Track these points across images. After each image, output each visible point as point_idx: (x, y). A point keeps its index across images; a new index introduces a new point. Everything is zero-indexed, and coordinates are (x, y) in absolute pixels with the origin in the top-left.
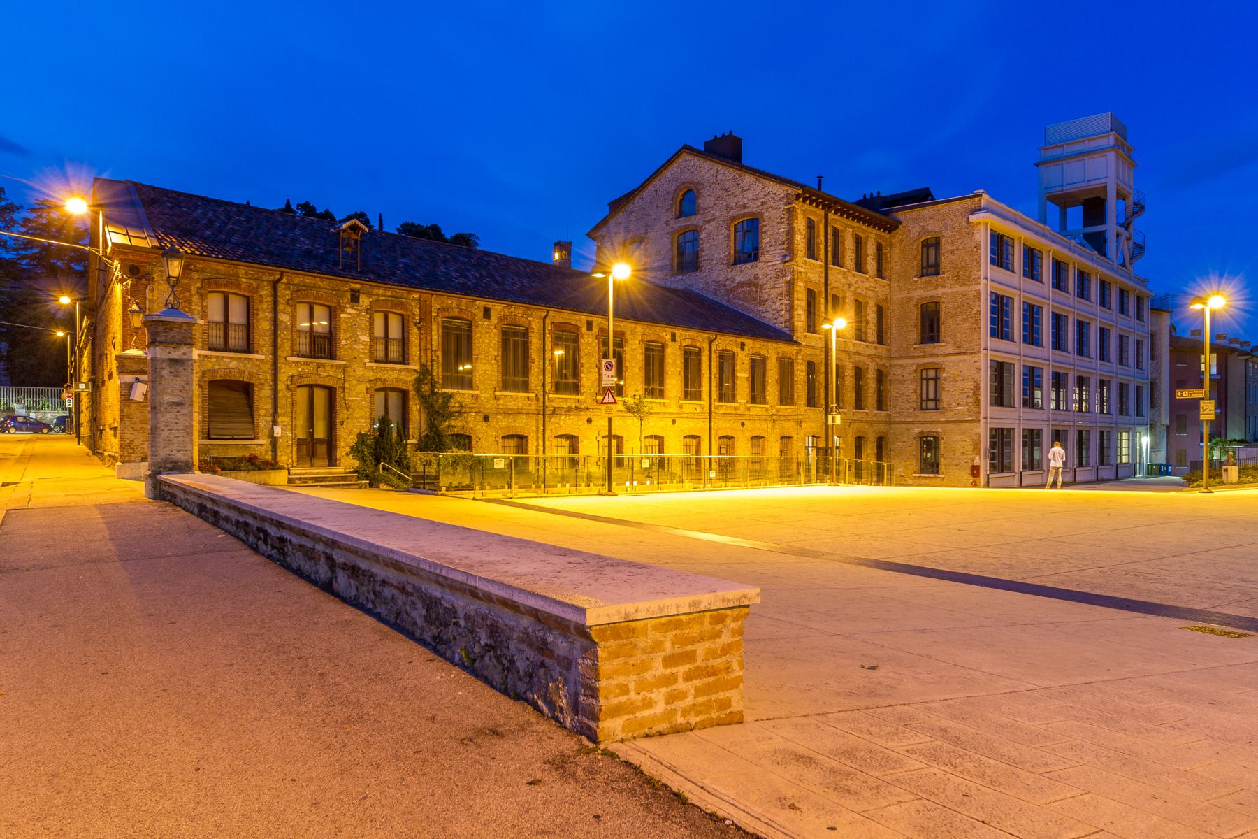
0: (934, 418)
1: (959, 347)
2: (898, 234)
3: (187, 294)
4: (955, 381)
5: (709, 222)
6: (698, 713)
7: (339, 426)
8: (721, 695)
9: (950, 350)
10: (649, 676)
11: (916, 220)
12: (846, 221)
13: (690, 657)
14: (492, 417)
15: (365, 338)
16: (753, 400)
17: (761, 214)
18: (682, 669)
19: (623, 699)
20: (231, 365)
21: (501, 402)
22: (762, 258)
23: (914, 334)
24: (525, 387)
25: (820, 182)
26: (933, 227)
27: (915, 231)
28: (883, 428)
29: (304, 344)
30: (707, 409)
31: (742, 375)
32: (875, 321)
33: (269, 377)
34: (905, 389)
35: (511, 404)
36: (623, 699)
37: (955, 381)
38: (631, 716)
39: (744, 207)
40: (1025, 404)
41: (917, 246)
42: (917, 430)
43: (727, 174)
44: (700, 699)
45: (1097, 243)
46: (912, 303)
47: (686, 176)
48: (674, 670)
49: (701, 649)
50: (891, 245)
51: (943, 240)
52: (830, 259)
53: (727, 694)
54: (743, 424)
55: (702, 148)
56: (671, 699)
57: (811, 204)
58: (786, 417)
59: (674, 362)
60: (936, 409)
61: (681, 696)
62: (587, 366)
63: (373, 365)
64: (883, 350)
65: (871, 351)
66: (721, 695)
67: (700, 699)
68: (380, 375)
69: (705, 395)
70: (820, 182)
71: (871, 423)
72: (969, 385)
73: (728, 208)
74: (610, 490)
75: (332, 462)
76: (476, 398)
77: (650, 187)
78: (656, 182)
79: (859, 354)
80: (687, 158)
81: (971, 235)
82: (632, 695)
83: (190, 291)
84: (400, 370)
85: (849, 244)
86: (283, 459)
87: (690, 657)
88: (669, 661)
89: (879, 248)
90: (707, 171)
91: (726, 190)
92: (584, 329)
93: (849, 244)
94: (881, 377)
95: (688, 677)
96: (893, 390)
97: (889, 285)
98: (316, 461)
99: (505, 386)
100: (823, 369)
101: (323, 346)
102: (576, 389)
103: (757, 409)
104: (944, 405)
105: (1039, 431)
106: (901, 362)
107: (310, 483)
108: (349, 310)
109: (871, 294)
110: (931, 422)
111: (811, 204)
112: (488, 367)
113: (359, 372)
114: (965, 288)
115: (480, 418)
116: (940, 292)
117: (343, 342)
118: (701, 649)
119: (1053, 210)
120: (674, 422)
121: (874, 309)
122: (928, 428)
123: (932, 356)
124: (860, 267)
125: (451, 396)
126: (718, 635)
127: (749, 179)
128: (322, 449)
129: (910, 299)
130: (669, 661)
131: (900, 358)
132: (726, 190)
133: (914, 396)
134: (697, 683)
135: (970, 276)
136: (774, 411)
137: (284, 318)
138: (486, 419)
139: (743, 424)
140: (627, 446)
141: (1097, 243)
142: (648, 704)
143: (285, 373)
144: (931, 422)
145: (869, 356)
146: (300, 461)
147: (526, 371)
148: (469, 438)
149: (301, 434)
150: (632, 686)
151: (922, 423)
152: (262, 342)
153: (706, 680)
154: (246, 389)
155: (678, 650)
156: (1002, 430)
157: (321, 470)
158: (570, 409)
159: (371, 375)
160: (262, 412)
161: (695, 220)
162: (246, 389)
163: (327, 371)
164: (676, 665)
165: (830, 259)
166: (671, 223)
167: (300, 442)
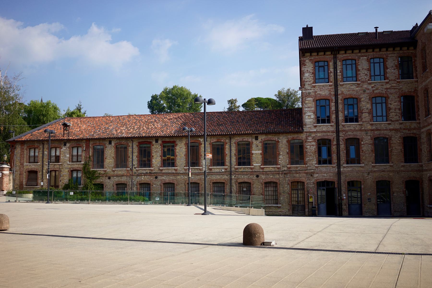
14: (112, 177)
20: (33, 167)
21: (116, 172)
31: (257, 152)
35: (120, 173)
50: (416, 57)
62: (155, 157)
64: (408, 123)
65: (397, 126)
68: (72, 166)
69: (227, 163)
76: (105, 171)
79: (380, 130)
84: (79, 164)
92: (154, 142)
99: (117, 166)
100: (335, 143)
102: (173, 164)
109: (393, 91)
113: (66, 166)
115: (107, 178)
125: (96, 171)
138: (109, 178)
139: (257, 176)
145: (391, 130)
148: (103, 185)
158: (147, 173)
159: (70, 166)
163: (57, 166)
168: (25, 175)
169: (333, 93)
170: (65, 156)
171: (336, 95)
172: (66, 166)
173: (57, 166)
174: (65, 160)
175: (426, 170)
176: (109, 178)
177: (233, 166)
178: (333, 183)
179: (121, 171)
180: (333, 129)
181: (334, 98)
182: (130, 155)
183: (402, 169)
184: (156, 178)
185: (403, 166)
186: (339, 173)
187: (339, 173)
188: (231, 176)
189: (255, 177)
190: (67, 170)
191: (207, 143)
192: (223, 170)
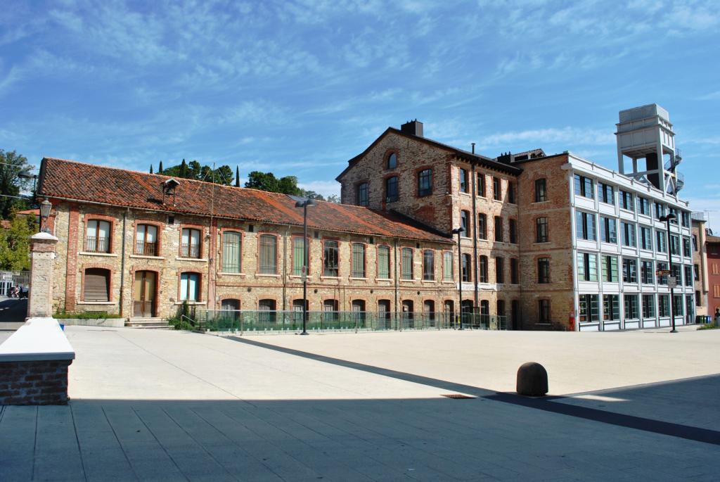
0: (546, 289)
1: (559, 245)
2: (522, 177)
3: (76, 222)
4: (557, 265)
5: (404, 171)
6: (43, 399)
7: (159, 294)
8: (56, 394)
9: (553, 246)
10: (18, 383)
11: (532, 169)
12: (487, 170)
13: (40, 378)
14: (253, 289)
15: (176, 244)
16: (426, 277)
17: (433, 166)
18: (35, 382)
19: (5, 390)
20: (100, 262)
22: (434, 193)
23: (532, 238)
24: (276, 271)
25: (473, 146)
26: (540, 172)
27: (531, 175)
28: (516, 295)
29: (140, 249)
30: (393, 284)
31: (418, 262)
32: (508, 229)
33: (120, 266)
34: (530, 271)
36: (5, 390)
37: (557, 265)
38: (9, 397)
39: (424, 162)
40: (625, 280)
41: (533, 184)
42: (537, 295)
43: (415, 144)
44: (44, 394)
45: (655, 181)
46: (531, 218)
47: (391, 145)
48: (31, 382)
49: (45, 375)
50: (518, 183)
51: (548, 181)
52: (476, 193)
53: (59, 394)
54: (419, 293)
55: (400, 128)
56: (29, 392)
57: (462, 160)
58: (431, 290)
59: (372, 256)
60: (548, 282)
61: (35, 392)
62: (314, 259)
63: (181, 259)
64: (514, 247)
65: (506, 247)
66: (56, 394)
67: (44, 394)
70: (473, 146)
71: (508, 292)
72: (566, 268)
73: (414, 163)
74: (304, 331)
75: (154, 314)
77: (371, 151)
78: (375, 149)
80: (391, 134)
81: (563, 177)
82: (10, 389)
83: (78, 220)
85: (489, 181)
86: (126, 312)
87: (40, 378)
88: (28, 378)
89: (510, 185)
90: (403, 142)
91: (413, 153)
93: (489, 181)
94: (514, 263)
95: (38, 385)
96: (522, 271)
97: (518, 208)
98: (146, 315)
99: (262, 269)
100: (472, 259)
101: (154, 249)
103: (428, 284)
104: (552, 280)
105: (617, 297)
106: (527, 254)
107: (140, 326)
108: (168, 228)
110: (545, 291)
111: (462, 160)
112: (252, 259)
113: (173, 263)
114: (561, 209)
115: (245, 289)
116: (547, 211)
117: (163, 246)
118: (45, 375)
119: (628, 161)
120: (372, 292)
121: (508, 222)
122: (543, 295)
123: (544, 250)
124: (497, 196)
126: (55, 370)
127: (426, 147)
128: (149, 307)
129: (529, 216)
130: (28, 378)
131: (525, 251)
132: (413, 153)
133: (534, 275)
134: (43, 388)
135: (563, 201)
136: (440, 285)
137: (129, 233)
138: (249, 290)
139: (419, 293)
140: (341, 307)
141: (655, 181)
142: (17, 393)
143: (128, 265)
144: (545, 291)
145: (505, 251)
146: (136, 313)
147: (276, 262)
149: (138, 298)
150: (10, 386)
151: (539, 291)
152: (116, 247)
153: (47, 387)
154: (106, 273)
155: (32, 374)
156: (590, 295)
157: (148, 318)
159: (179, 265)
160: (115, 286)
161: (385, 173)
162: (106, 273)
164: (32, 380)
165: (476, 193)
166: (383, 172)
167: (136, 303)
168: (79, 278)
169: (471, 205)
170: (171, 244)
171: (474, 208)
172: (173, 263)
173: (153, 265)
174: (170, 253)
175: (528, 291)
176: (249, 290)
177: (398, 279)
178: (471, 302)
179: (268, 278)
180: (471, 244)
181: (471, 211)
182: (281, 252)
183: (510, 289)
184: (316, 291)
185: (510, 287)
186: (476, 292)
187: (476, 292)
188: (396, 292)
189: (417, 295)
190: (174, 272)
191: (397, 248)
192: (389, 284)
